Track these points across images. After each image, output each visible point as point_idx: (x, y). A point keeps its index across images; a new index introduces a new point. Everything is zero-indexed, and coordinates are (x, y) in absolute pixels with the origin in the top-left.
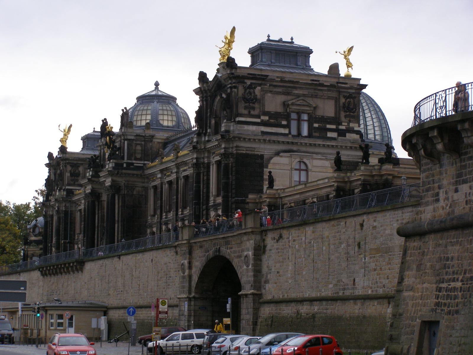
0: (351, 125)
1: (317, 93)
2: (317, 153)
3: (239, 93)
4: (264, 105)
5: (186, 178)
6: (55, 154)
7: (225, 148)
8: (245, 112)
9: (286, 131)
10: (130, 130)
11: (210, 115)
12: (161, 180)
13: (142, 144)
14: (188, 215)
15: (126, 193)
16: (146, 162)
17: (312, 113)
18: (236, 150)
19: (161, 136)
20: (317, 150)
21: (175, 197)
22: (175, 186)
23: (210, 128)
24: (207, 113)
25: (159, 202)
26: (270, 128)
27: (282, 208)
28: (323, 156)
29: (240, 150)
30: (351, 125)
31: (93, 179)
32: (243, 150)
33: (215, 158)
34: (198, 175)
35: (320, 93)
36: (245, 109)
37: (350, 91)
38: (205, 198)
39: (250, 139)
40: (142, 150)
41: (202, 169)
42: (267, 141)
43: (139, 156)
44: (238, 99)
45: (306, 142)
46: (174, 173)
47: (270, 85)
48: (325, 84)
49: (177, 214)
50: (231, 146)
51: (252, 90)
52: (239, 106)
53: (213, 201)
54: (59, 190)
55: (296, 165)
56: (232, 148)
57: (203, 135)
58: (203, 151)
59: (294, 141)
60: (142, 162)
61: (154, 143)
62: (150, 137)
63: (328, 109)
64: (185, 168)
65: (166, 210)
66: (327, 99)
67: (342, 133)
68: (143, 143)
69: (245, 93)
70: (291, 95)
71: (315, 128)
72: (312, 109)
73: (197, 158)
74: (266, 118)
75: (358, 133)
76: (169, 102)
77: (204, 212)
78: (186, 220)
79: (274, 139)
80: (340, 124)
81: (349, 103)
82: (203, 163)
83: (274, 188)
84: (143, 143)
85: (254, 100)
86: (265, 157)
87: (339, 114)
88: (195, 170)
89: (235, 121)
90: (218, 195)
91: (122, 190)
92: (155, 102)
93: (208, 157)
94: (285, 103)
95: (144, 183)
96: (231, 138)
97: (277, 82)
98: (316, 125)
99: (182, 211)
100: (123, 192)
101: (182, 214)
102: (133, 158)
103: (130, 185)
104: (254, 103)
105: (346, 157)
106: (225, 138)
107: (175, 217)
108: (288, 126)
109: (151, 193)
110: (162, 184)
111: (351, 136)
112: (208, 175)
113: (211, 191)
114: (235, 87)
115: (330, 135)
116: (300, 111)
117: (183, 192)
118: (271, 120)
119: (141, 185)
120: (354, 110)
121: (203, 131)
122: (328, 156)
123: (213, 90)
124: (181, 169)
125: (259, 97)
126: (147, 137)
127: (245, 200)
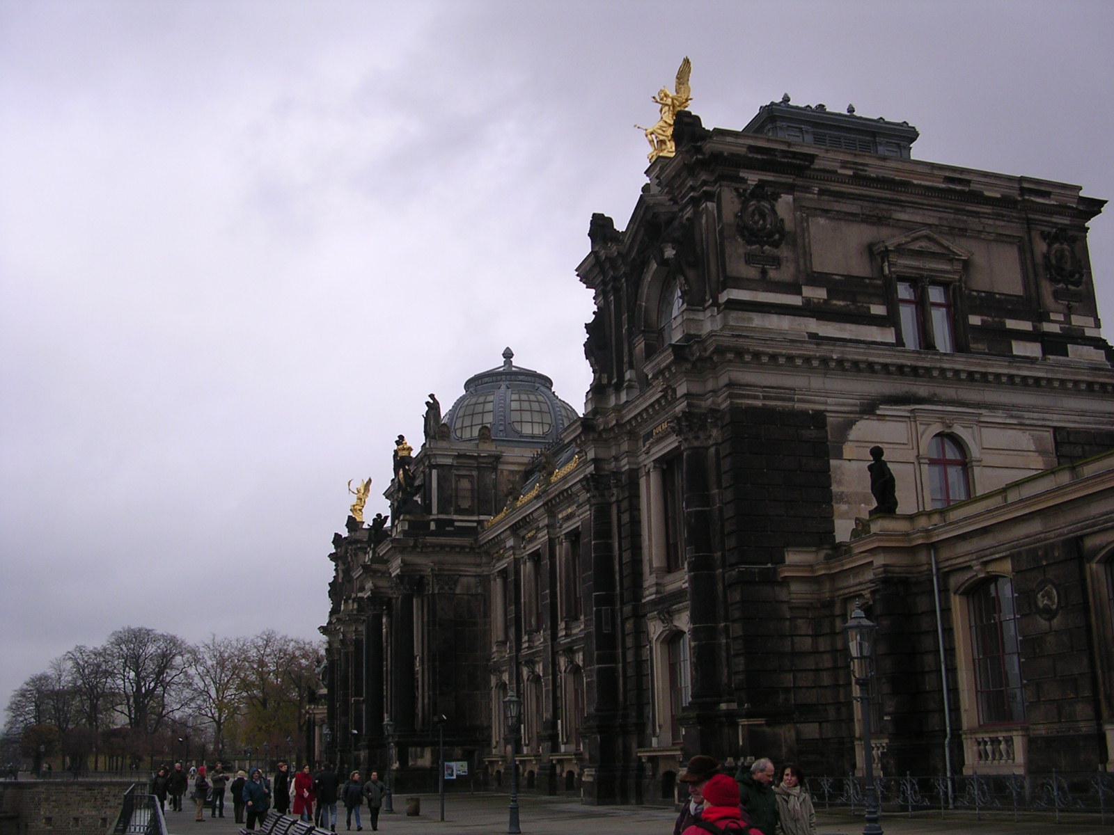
0: (1076, 320)
1: (965, 221)
2: (992, 407)
3: (724, 212)
4: (807, 255)
5: (574, 536)
6: (345, 533)
7: (687, 395)
8: (752, 272)
9: (889, 336)
10: (444, 444)
11: (629, 329)
12: (514, 554)
13: (472, 476)
14: (582, 638)
15: (436, 592)
16: (482, 517)
17: (960, 280)
18: (730, 396)
19: (517, 457)
20: (991, 396)
21: (548, 591)
22: (546, 562)
23: (631, 367)
24: (619, 325)
25: (513, 607)
26: (838, 325)
27: (944, 590)
28: (1012, 417)
29: (743, 396)
30: (1076, 320)
31: (375, 566)
32: (756, 397)
33: (653, 451)
34: (602, 513)
35: (973, 223)
36: (748, 262)
37: (1056, 219)
38: (627, 582)
39: (774, 357)
40: (472, 490)
41: (615, 491)
42: (833, 364)
43: (465, 504)
44: (721, 232)
45: (958, 367)
46: (543, 528)
47: (822, 192)
48: (987, 193)
49: (554, 636)
50: (710, 385)
51: (766, 204)
52: (728, 251)
53: (653, 590)
54: (346, 602)
55: (927, 444)
56: (714, 391)
57: (611, 390)
58: (615, 438)
59: (920, 364)
60: (475, 518)
61: (502, 472)
62: (491, 460)
63: (1001, 272)
64: (570, 510)
65: (531, 625)
66: (994, 240)
67: (1054, 345)
68: (475, 473)
69: (744, 209)
70: (888, 225)
71: (974, 327)
72: (958, 266)
73: (596, 461)
74: (820, 294)
75: (1100, 343)
76: (534, 386)
77: (629, 626)
78: (578, 651)
79: (857, 357)
80: (1044, 317)
81: (1061, 257)
82: (616, 474)
83: (898, 511)
84: (475, 473)
85: (777, 236)
86: (831, 419)
87: (1037, 286)
88: (594, 497)
89: (715, 303)
90: (671, 565)
91: (428, 584)
92: (503, 387)
93: (632, 453)
94: (875, 248)
95: (479, 565)
96: (710, 358)
97: (843, 180)
98: (975, 320)
99: (567, 628)
100: (429, 590)
101: (566, 636)
102: (452, 509)
103: (446, 573)
104: (776, 245)
105: (1077, 418)
106: (687, 360)
107: (550, 643)
108: (891, 320)
109: (497, 586)
110: (517, 562)
111: (1079, 353)
112: (634, 508)
113: (646, 557)
114: (709, 196)
115: (1019, 348)
116: (925, 273)
117: (568, 576)
118: (835, 302)
119: (473, 570)
120: (1077, 276)
121: (610, 379)
122: (1026, 415)
123: (633, 254)
124: (560, 516)
125: (789, 226)
126: (481, 460)
127: (775, 571)
